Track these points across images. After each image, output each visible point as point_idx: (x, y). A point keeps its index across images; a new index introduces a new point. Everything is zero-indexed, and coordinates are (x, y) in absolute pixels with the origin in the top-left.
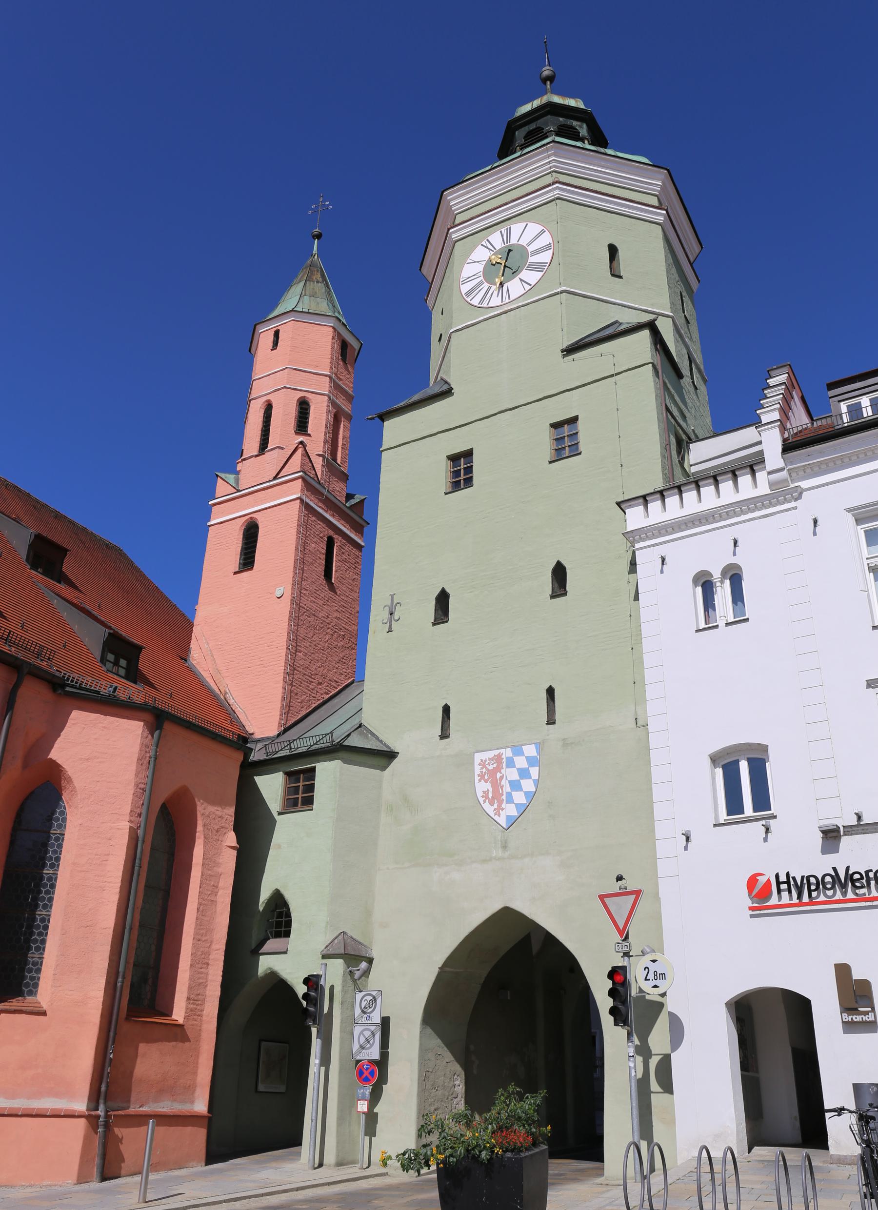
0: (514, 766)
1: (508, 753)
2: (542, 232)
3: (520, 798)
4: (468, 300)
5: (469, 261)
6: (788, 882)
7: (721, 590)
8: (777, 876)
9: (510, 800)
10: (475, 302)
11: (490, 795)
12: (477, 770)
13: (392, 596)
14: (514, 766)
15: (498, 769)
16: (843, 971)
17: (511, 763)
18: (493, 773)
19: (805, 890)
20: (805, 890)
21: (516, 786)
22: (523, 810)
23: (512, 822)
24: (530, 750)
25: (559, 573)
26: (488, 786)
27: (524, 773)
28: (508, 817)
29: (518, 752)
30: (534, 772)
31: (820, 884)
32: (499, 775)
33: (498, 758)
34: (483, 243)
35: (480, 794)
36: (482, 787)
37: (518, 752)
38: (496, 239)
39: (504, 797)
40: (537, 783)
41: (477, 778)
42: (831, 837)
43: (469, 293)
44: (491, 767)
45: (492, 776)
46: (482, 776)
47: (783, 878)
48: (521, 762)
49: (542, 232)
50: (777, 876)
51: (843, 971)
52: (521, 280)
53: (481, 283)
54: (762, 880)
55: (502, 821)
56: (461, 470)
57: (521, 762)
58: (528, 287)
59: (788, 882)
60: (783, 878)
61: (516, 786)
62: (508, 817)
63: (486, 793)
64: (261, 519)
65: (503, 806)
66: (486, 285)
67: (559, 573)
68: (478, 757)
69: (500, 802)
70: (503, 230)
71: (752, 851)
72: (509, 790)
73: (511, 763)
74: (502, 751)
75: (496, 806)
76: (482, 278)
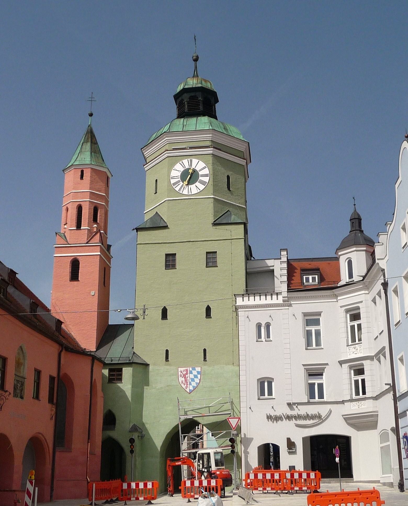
1: (191, 369)
2: (204, 168)
3: (194, 384)
7: (263, 330)
9: (190, 384)
10: (177, 189)
12: (179, 373)
13: (144, 305)
15: (187, 374)
17: (191, 373)
21: (193, 380)
22: (195, 388)
23: (191, 392)
24: (198, 369)
25: (208, 310)
26: (183, 379)
27: (196, 376)
29: (194, 369)
30: (199, 376)
32: (187, 376)
33: (187, 370)
35: (180, 382)
36: (181, 379)
37: (194, 369)
38: (186, 162)
39: (188, 383)
40: (200, 380)
43: (174, 184)
44: (184, 373)
45: (184, 376)
46: (181, 376)
48: (195, 373)
49: (204, 168)
53: (179, 181)
55: (188, 390)
56: (170, 261)
57: (195, 373)
61: (193, 380)
65: (188, 386)
66: (181, 183)
67: (208, 310)
68: (180, 369)
69: (187, 385)
73: (191, 373)
75: (186, 386)
76: (180, 179)
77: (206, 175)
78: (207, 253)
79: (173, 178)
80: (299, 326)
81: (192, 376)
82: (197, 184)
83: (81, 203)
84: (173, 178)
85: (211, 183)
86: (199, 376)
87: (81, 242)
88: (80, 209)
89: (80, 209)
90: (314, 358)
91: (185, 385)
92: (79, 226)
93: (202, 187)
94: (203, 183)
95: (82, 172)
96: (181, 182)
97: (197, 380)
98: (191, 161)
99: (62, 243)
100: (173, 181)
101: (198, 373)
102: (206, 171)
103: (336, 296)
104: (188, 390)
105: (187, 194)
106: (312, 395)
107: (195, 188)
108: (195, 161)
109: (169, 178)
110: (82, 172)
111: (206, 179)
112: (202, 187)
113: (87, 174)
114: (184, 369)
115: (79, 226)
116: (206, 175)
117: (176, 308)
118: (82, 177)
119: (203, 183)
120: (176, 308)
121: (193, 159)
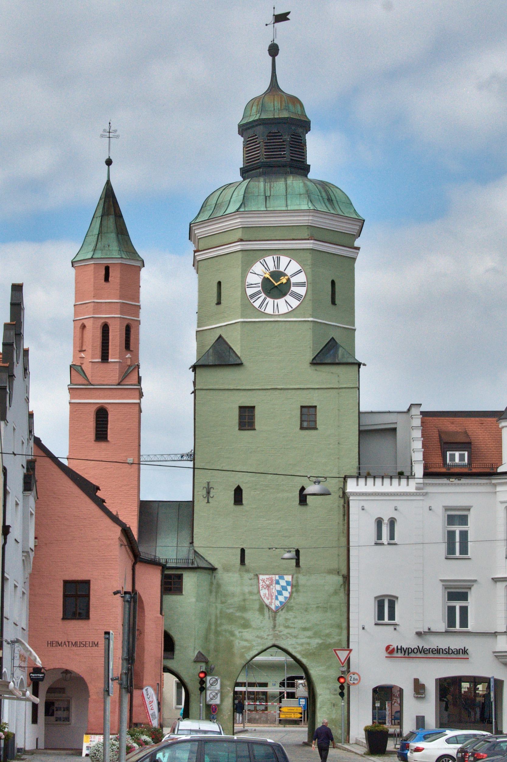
0: (279, 584)
1: (277, 577)
4: (252, 301)
5: (251, 271)
6: (401, 649)
8: (397, 647)
9: (277, 598)
10: (257, 304)
11: (267, 595)
14: (279, 584)
16: (416, 681)
17: (277, 583)
18: (268, 587)
19: (407, 653)
20: (407, 653)
21: (280, 593)
24: (288, 578)
28: (276, 607)
29: (282, 578)
31: (413, 651)
34: (261, 261)
38: (269, 260)
39: (274, 597)
41: (261, 587)
42: (419, 634)
43: (252, 296)
44: (268, 583)
47: (399, 647)
48: (283, 583)
50: (397, 647)
51: (416, 681)
52: (286, 302)
53: (258, 293)
54: (391, 648)
58: (290, 309)
59: (401, 649)
60: (399, 647)
61: (280, 593)
62: (276, 607)
63: (265, 595)
64: (110, 410)
65: (274, 601)
69: (272, 599)
70: (275, 257)
71: (387, 636)
72: (276, 594)
73: (277, 583)
74: (274, 576)
76: (260, 288)
77: (301, 284)
78: (302, 407)
79: (250, 286)
80: (437, 527)
81: (278, 587)
82: (288, 298)
83: (107, 320)
84: (250, 286)
85: (309, 297)
86: (289, 588)
87: (110, 382)
88: (105, 329)
89: (105, 329)
90: (457, 571)
91: (268, 599)
92: (105, 357)
93: (295, 303)
94: (296, 296)
95: (107, 269)
96: (263, 294)
97: (286, 594)
98: (279, 259)
99: (80, 382)
100: (250, 291)
101: (288, 583)
102: (302, 278)
103: (495, 485)
104: (273, 607)
105: (272, 313)
106: (451, 623)
107: (284, 305)
108: (284, 260)
109: (244, 286)
110: (107, 269)
111: (302, 291)
112: (295, 303)
113: (114, 274)
114: (267, 576)
115: (105, 357)
116: (301, 284)
117: (255, 489)
118: (107, 279)
119: (296, 296)
120: (255, 489)
121: (281, 257)
